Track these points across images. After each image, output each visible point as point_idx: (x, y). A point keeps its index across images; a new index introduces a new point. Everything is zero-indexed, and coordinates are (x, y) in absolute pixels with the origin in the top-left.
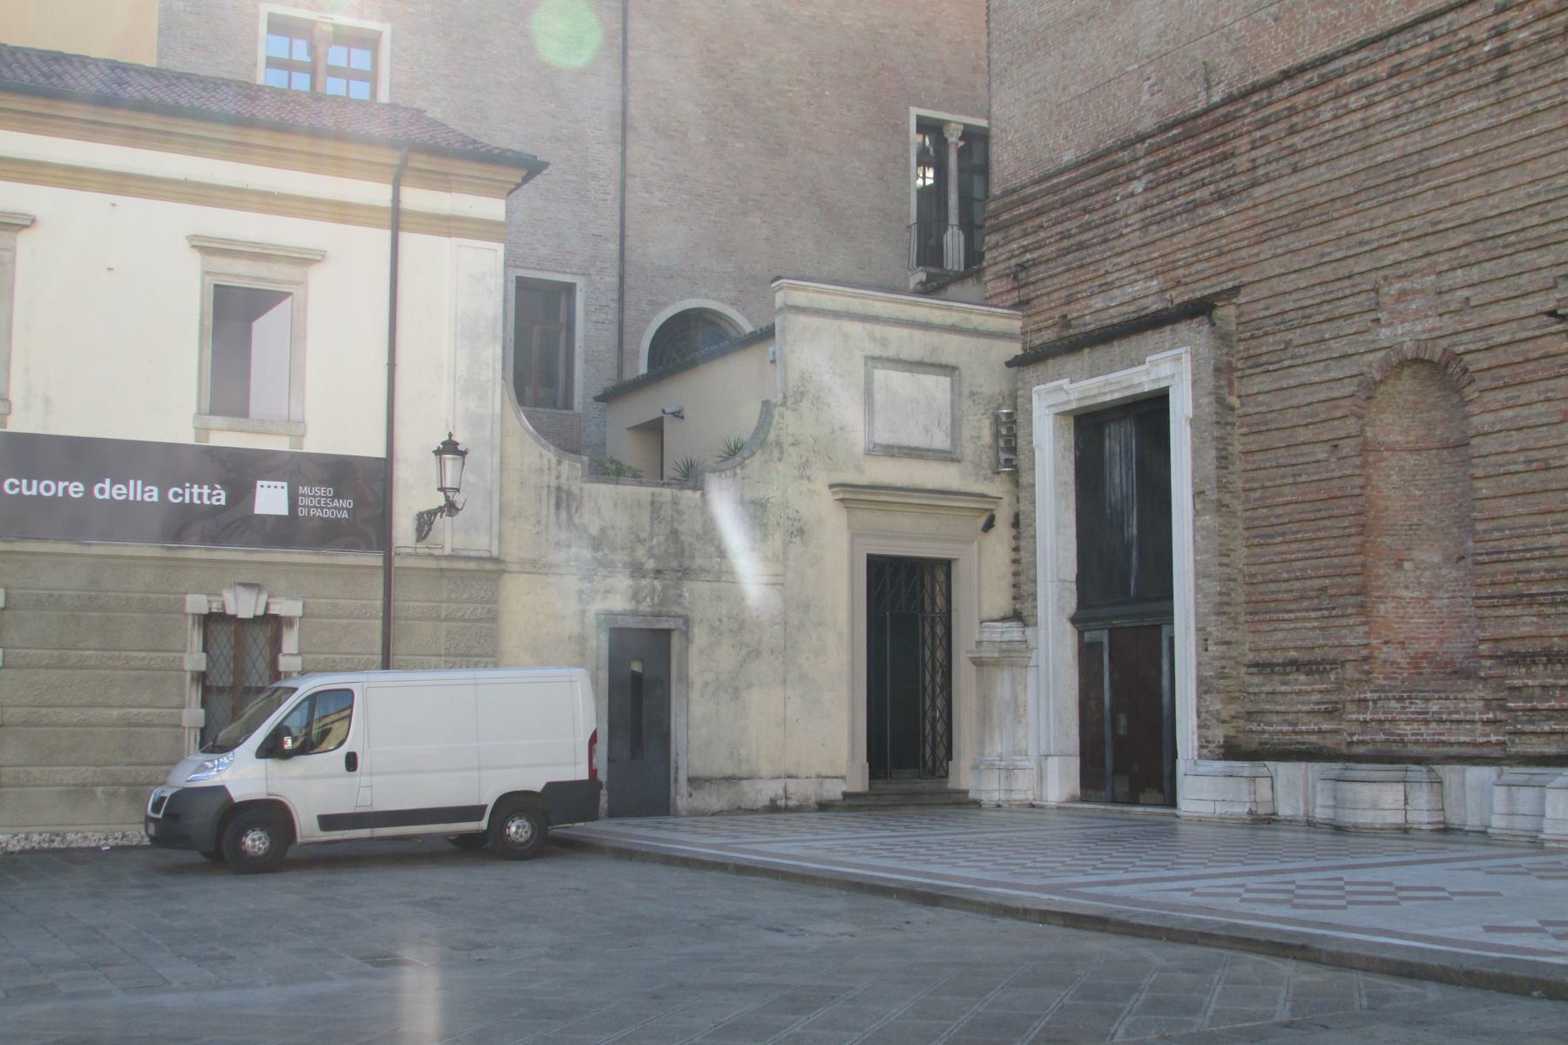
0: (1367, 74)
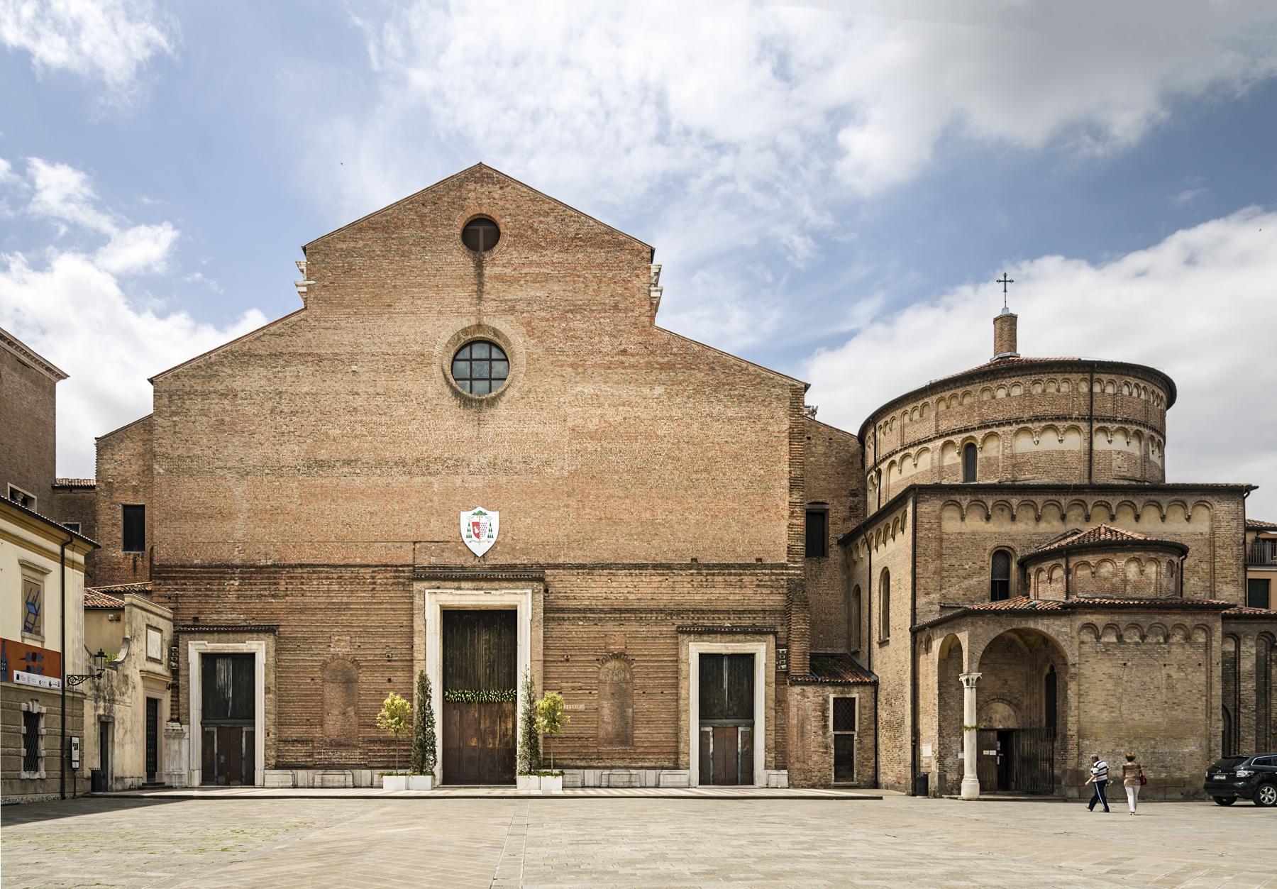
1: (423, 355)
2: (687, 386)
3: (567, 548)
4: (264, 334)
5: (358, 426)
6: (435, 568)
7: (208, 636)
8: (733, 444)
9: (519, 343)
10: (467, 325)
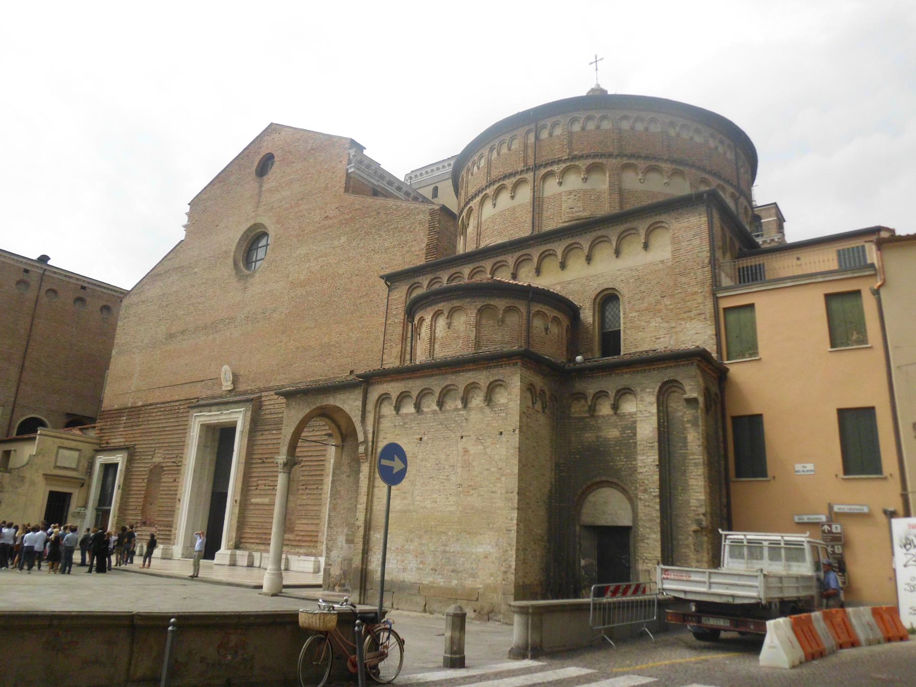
1: (226, 252)
2: (361, 231)
7: (105, 453)
8: (387, 268)
9: (272, 229)
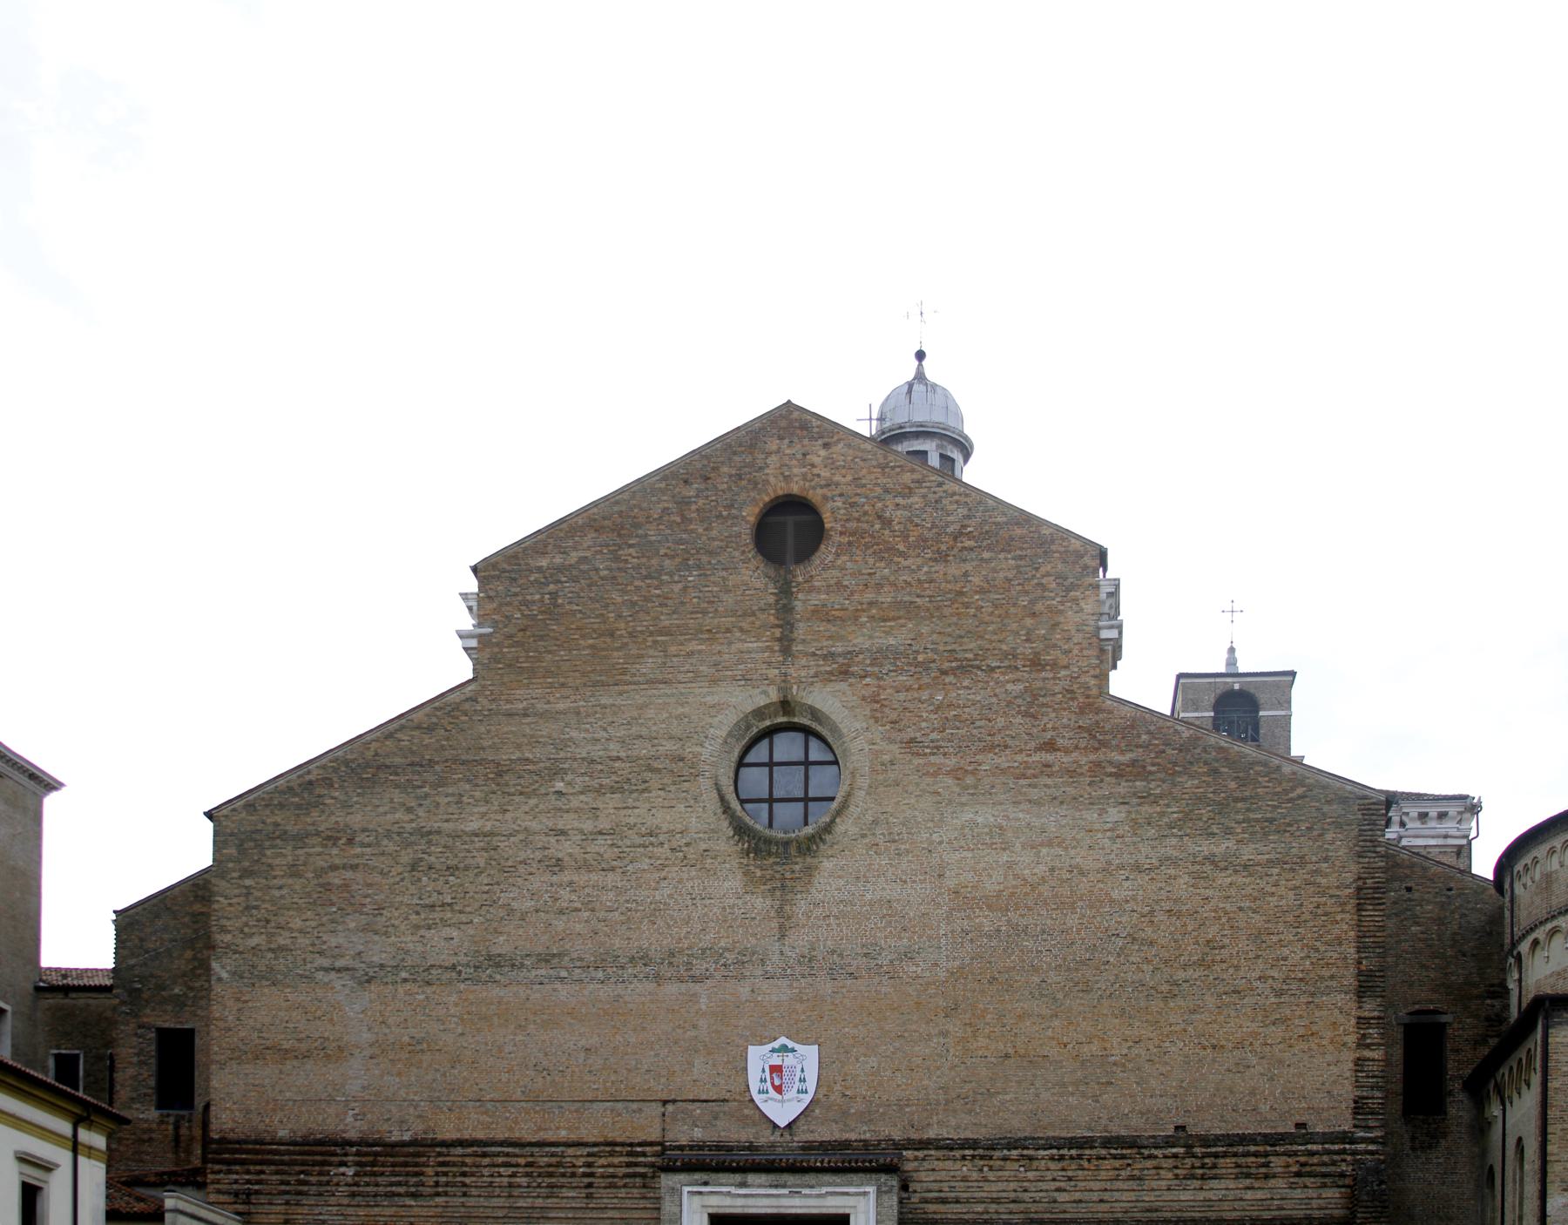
0: (513, 1160)
2: (1168, 806)
3: (945, 1110)
4: (402, 727)
5: (565, 894)
6: (701, 1148)
10: (762, 701)
